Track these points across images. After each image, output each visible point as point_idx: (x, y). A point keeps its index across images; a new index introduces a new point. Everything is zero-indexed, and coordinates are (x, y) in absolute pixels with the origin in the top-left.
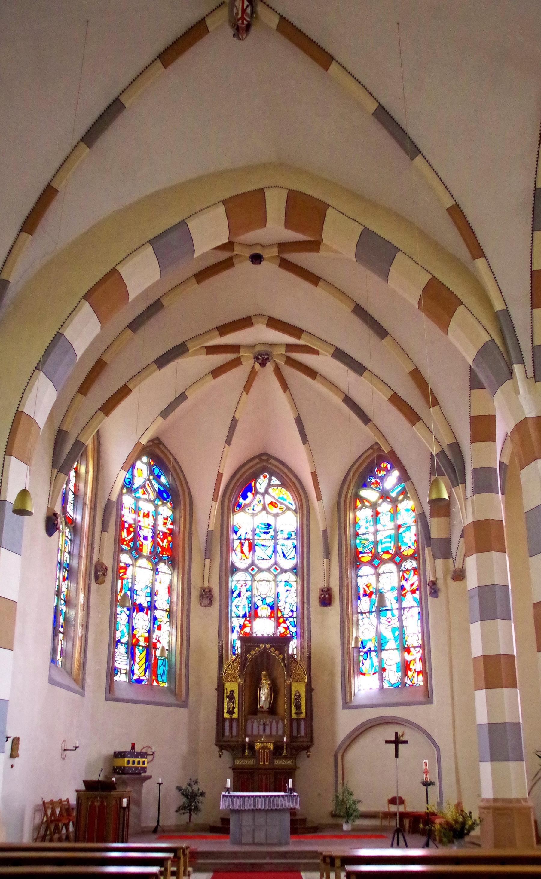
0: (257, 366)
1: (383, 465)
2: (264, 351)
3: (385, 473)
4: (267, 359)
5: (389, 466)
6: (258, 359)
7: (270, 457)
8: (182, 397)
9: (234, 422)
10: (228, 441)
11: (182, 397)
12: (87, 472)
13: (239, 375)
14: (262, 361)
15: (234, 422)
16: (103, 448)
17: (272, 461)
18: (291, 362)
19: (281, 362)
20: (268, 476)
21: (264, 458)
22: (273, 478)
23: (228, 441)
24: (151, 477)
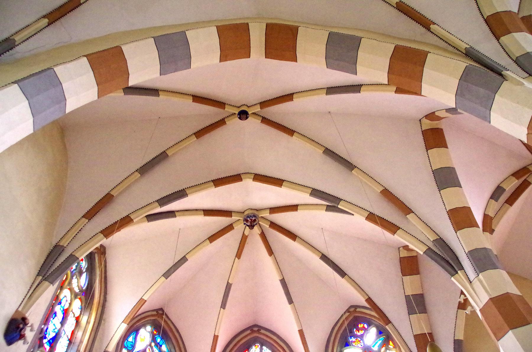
0: (247, 231)
1: (360, 326)
2: (252, 213)
3: (363, 331)
4: (255, 220)
5: (366, 326)
6: (247, 221)
7: (260, 328)
8: (184, 260)
9: (229, 287)
10: (223, 305)
11: (184, 260)
12: (88, 322)
13: (231, 240)
14: (251, 222)
15: (229, 287)
16: (107, 304)
17: (262, 331)
18: (274, 225)
19: (266, 226)
20: (259, 346)
21: (256, 329)
22: (264, 347)
23: (223, 305)
24: (153, 344)
